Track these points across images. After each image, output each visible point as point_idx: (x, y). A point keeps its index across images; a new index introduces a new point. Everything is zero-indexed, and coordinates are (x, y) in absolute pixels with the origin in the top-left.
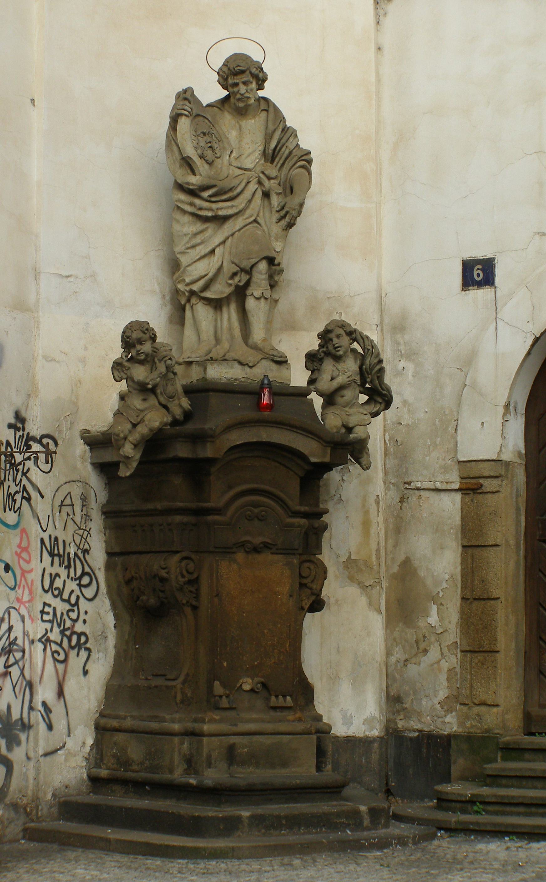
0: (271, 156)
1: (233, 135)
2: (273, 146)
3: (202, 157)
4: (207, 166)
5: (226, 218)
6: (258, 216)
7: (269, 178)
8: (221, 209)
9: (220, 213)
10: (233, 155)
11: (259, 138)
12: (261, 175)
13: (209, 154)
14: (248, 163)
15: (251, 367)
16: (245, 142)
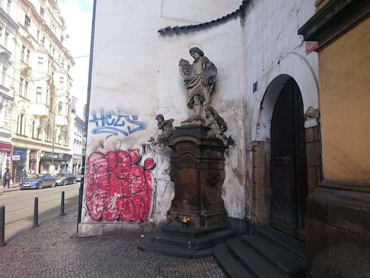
0: (205, 69)
1: (195, 67)
2: (204, 67)
3: (185, 74)
4: (187, 76)
5: (192, 87)
6: (200, 85)
7: (202, 75)
8: (189, 85)
9: (189, 86)
10: (196, 72)
11: (201, 66)
12: (200, 75)
13: (187, 73)
14: (198, 73)
15: (191, 122)
16: (198, 69)
